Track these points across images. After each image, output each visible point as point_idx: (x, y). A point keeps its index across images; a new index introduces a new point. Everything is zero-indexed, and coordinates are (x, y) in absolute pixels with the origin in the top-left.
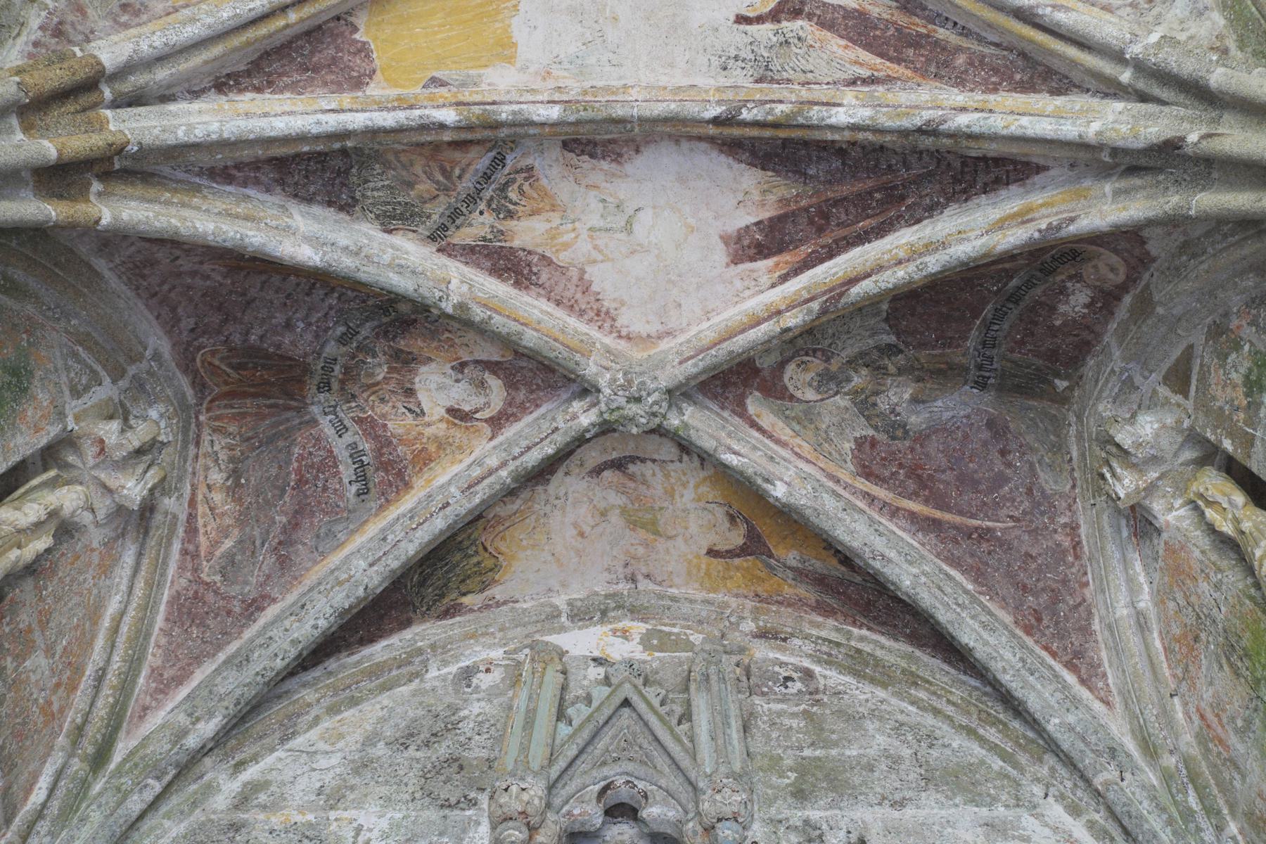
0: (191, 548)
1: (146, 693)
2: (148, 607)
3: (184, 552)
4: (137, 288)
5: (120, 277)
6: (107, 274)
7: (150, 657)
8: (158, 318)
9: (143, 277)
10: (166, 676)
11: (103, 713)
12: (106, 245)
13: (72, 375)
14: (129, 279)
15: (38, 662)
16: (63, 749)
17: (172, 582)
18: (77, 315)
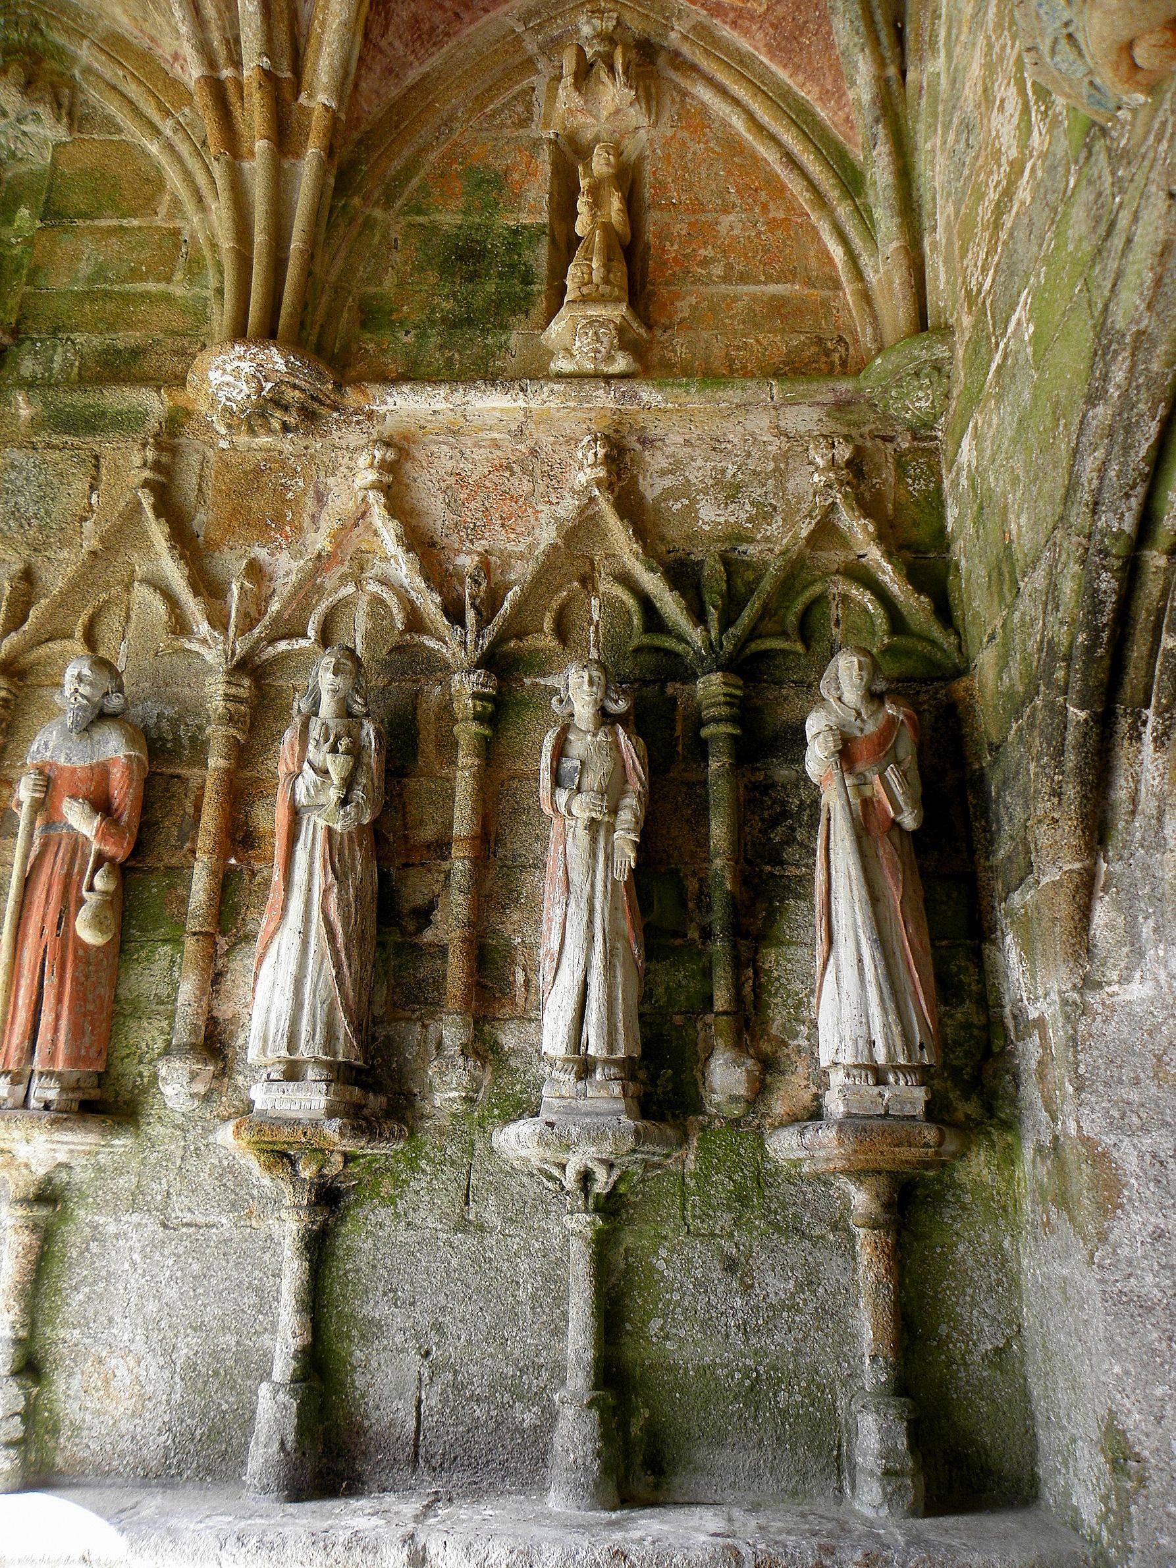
0: (732, 15)
1: (835, 113)
2: (763, 86)
3: (734, 24)
4: (448, 34)
5: (432, 54)
6: (426, 68)
7: (808, 98)
8: (486, 11)
9: (433, 29)
10: (829, 87)
11: (818, 169)
12: (391, 71)
13: (509, 122)
14: (434, 44)
15: (730, 224)
16: (819, 219)
17: (756, 48)
18: (455, 108)
